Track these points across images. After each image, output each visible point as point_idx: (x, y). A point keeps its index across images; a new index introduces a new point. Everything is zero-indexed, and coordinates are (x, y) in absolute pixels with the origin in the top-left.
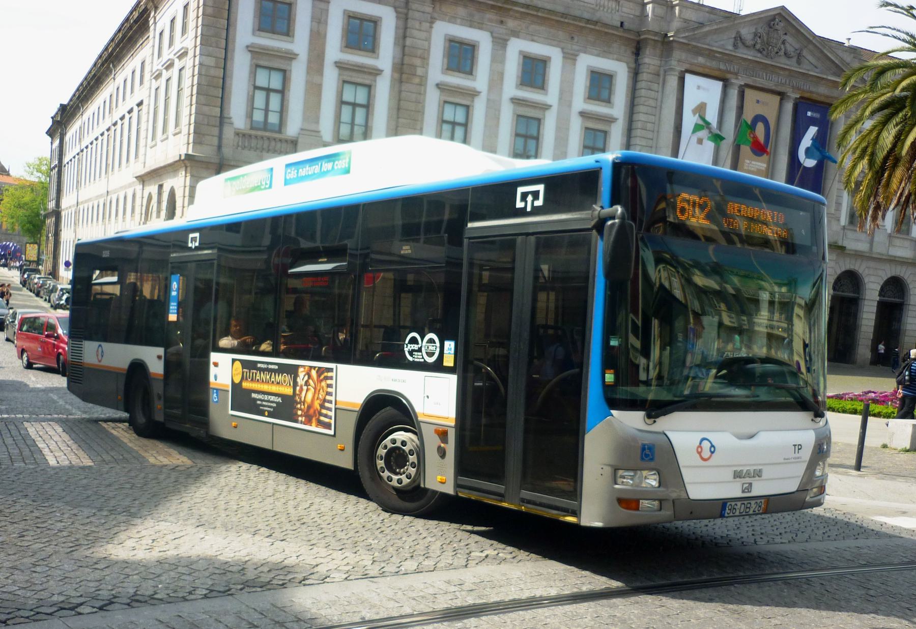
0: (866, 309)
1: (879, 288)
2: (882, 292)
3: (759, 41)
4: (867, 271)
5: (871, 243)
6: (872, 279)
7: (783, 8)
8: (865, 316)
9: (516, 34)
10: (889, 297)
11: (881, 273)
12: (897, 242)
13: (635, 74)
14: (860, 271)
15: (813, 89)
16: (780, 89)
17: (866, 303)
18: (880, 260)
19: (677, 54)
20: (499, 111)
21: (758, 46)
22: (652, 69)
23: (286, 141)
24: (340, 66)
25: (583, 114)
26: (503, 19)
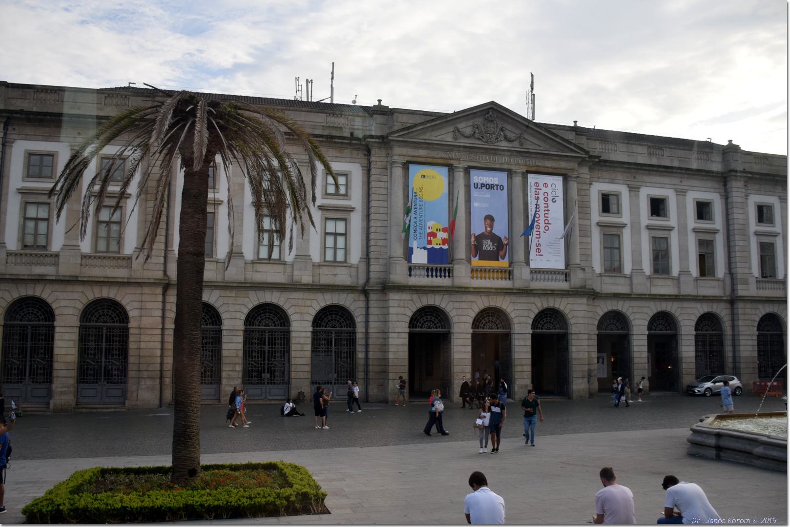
0: (635, 343)
1: (646, 323)
3: (477, 131)
5: (631, 285)
6: (638, 316)
7: (493, 103)
8: (635, 349)
10: (661, 330)
11: (645, 310)
12: (660, 282)
14: (624, 311)
16: (506, 167)
17: (635, 337)
18: (642, 297)
20: (242, 214)
21: (477, 135)
22: (379, 165)
23: (124, 258)
24: (23, 192)
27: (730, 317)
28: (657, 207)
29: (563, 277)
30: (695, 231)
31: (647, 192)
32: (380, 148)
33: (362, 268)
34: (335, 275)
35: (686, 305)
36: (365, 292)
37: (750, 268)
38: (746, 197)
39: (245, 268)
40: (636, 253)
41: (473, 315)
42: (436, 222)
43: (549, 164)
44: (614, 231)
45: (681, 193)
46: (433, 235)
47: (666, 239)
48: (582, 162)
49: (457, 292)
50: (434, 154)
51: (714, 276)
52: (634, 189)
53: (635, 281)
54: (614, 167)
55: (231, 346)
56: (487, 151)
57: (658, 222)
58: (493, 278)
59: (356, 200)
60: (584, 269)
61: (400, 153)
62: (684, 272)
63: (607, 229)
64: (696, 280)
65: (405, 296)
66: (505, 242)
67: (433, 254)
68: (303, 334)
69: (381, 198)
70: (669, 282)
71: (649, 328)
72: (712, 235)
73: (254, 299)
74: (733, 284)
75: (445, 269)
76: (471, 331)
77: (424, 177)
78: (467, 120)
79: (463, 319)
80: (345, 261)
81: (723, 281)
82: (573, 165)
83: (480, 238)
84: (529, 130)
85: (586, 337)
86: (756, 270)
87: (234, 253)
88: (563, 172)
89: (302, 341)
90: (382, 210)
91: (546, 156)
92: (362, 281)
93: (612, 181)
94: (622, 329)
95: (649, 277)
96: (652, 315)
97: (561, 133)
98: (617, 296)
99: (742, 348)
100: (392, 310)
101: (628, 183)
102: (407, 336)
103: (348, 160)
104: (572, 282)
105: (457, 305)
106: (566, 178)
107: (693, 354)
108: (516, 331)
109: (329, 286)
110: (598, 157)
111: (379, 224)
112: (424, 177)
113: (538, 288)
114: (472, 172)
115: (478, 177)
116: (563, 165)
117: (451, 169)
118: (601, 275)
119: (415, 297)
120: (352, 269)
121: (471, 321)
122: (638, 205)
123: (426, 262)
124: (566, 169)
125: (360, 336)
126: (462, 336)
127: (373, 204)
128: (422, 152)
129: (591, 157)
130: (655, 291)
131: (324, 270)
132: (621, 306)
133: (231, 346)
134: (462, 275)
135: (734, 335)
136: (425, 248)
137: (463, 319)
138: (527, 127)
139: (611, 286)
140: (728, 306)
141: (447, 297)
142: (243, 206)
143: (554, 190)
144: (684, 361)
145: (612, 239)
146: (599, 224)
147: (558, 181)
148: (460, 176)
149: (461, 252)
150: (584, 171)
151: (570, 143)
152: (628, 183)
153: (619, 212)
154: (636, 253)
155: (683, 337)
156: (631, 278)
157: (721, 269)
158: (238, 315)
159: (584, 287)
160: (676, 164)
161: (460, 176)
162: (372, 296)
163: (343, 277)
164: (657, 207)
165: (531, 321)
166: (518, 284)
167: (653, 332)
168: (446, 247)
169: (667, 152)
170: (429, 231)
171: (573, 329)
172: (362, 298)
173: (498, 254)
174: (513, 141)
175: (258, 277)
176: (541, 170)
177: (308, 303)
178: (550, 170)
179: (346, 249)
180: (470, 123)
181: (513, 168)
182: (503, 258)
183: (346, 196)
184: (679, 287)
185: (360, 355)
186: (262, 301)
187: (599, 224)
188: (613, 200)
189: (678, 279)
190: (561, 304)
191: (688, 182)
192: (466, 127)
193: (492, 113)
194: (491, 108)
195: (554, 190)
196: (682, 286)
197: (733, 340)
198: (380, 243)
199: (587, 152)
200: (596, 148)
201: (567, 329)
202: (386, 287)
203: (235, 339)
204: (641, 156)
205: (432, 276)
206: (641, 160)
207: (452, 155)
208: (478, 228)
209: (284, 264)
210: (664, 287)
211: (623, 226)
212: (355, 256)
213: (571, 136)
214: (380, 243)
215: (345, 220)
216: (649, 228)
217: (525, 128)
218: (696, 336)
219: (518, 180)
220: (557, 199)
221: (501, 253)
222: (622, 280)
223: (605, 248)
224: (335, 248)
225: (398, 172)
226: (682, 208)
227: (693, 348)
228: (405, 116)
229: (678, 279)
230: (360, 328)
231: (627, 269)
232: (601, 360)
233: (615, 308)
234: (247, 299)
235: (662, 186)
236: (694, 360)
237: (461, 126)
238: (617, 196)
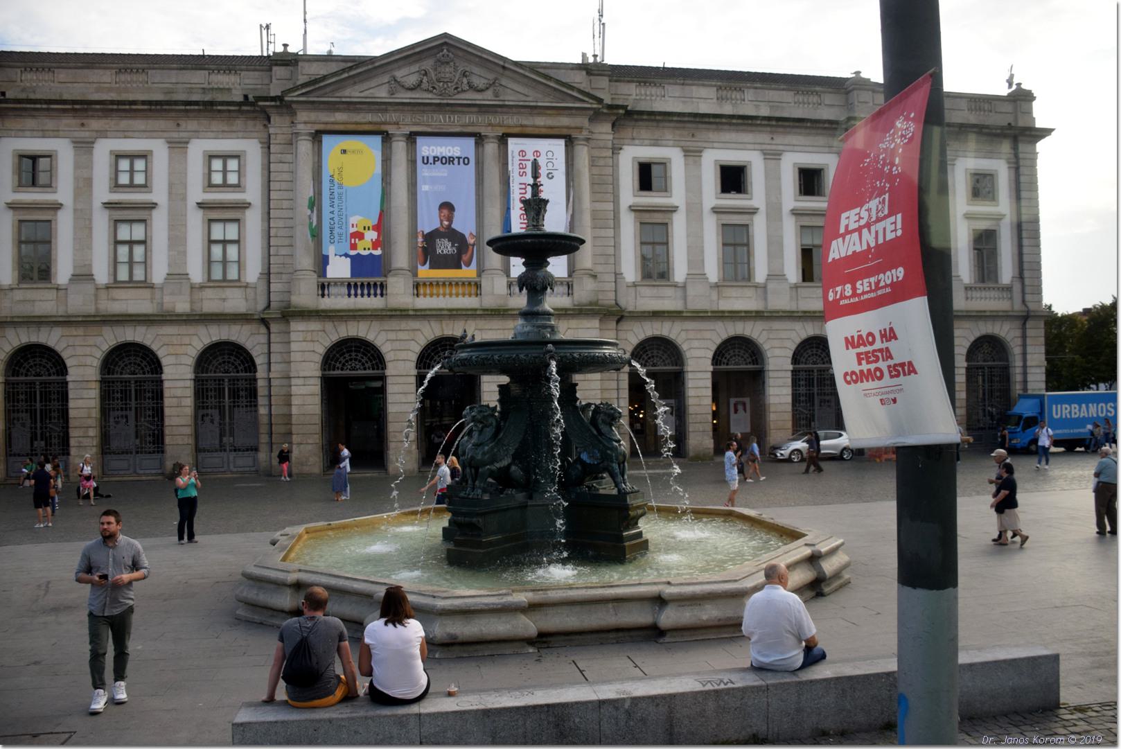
1: (710, 354)
2: (796, 359)
4: (683, 335)
5: (685, 298)
6: (696, 344)
7: (446, 35)
9: (103, 134)
10: (736, 364)
11: (708, 335)
12: (733, 292)
13: (267, 145)
15: (525, 122)
19: (302, 116)
20: (90, 220)
21: (425, 85)
22: (280, 139)
25: (201, 205)
26: (84, 121)
27: (1019, 341)
28: (733, 179)
30: (716, 211)
31: (714, 157)
32: (281, 114)
33: (262, 288)
34: (224, 300)
35: (777, 325)
36: (265, 322)
38: (616, 150)
39: (96, 296)
40: (695, 249)
41: (418, 349)
42: (361, 218)
43: (541, 121)
44: (658, 218)
45: (772, 156)
46: (360, 236)
47: (49, 221)
48: (596, 116)
49: (118, 321)
50: (359, 117)
51: (997, 282)
52: (693, 154)
53: (691, 291)
54: (658, 121)
55: (80, 403)
56: (440, 107)
57: (733, 200)
58: (451, 295)
59: (253, 193)
60: (595, 277)
61: (306, 120)
62: (776, 276)
63: (647, 215)
64: (796, 287)
65: (314, 325)
66: (471, 241)
67: (359, 263)
68: (181, 384)
69: (284, 186)
70: (749, 292)
71: (968, 360)
72: (146, 212)
73: (110, 338)
75: (369, 284)
77: (344, 152)
78: (410, 64)
79: (403, 355)
80: (239, 280)
82: (583, 121)
83: (431, 237)
84: (507, 73)
87: (83, 276)
88: (565, 132)
89: (179, 393)
90: (286, 204)
91: (534, 110)
92: (261, 305)
93: (656, 143)
94: (755, 362)
95: (717, 286)
96: (719, 341)
97: (552, 73)
98: (656, 315)
100: (294, 346)
101: (683, 144)
102: (318, 382)
103: (240, 134)
104: (576, 294)
105: (392, 336)
106: (570, 141)
107: (789, 399)
108: (689, 369)
109: (217, 315)
110: (624, 107)
111: (281, 223)
112: (344, 152)
113: (345, 307)
114: (420, 140)
115: (427, 148)
116: (565, 121)
117: (387, 138)
118: (635, 285)
119: (329, 326)
120: (249, 290)
121: (414, 357)
122: (699, 178)
123: (349, 275)
124: (568, 128)
125: (261, 383)
126: (699, 375)
127: (273, 195)
128: (340, 117)
129: (610, 107)
130: (725, 305)
131: (208, 293)
132: (52, 338)
133: (80, 403)
134: (399, 292)
136: (346, 255)
137: (403, 355)
138: (504, 67)
139: (650, 299)
140: (1018, 323)
141: (376, 325)
142: (91, 210)
143: (550, 161)
144: (772, 409)
145: (655, 230)
146: (634, 209)
147: (558, 146)
148: (400, 147)
149: (401, 257)
150: (604, 131)
151: (572, 88)
152: (683, 144)
153: (666, 189)
154: (695, 249)
155: (771, 374)
156: (684, 287)
158: (89, 360)
159: (596, 303)
160: (764, 111)
161: (400, 147)
162: (274, 327)
163: (235, 302)
164: (733, 179)
166: (488, 301)
168: (378, 252)
169: (749, 94)
170: (352, 230)
172: (263, 330)
173: (459, 259)
174: (481, 91)
175: (117, 308)
176: (529, 131)
177: (186, 340)
178: (544, 131)
179: (240, 263)
180: (415, 68)
181: (483, 131)
182: (468, 265)
183: (145, 187)
184: (766, 299)
185: (263, 411)
186: (121, 340)
187: (634, 209)
188: (655, 171)
191: (781, 140)
192: (408, 75)
193: (444, 51)
194: (445, 43)
195: (550, 161)
196: (770, 296)
198: (283, 251)
199: (600, 101)
200: (632, 95)
202: (289, 314)
203: (85, 394)
204: (705, 101)
205: (356, 295)
206: (704, 108)
207: (387, 117)
208: (429, 221)
209: (152, 287)
211: (672, 210)
212: (253, 273)
213: (579, 79)
214: (283, 251)
215: (144, 221)
216: (716, 211)
217: (501, 70)
218: (794, 372)
219: (491, 148)
220: (555, 173)
221: (465, 258)
222: (669, 292)
223: (724, 245)
224: (131, 263)
225: (305, 147)
226: (773, 179)
227: (789, 391)
228: (315, 65)
230: (261, 373)
231: (680, 272)
232: (740, 407)
234: (101, 338)
235: (741, 146)
236: (789, 408)
237: (399, 74)
238: (664, 164)
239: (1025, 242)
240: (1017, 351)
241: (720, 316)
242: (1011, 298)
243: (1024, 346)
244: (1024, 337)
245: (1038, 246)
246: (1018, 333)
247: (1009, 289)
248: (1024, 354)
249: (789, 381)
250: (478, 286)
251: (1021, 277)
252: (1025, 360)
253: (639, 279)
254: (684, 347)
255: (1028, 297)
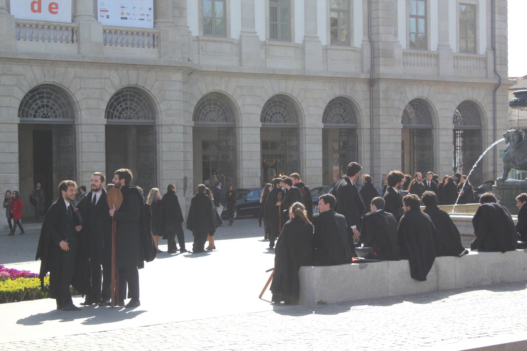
1: (259, 111)
10: (277, 121)
17: (244, 131)
29: (148, 40)
37: (396, 34)
41: (21, 96)
64: (326, 49)
74: (374, 57)
76: (17, 120)
81: (361, 52)
85: (181, 129)
86: (402, 40)
95: (264, 44)
96: (267, 99)
99: (382, 147)
135: (372, 129)
155: (308, 131)
157: (359, 37)
165: (104, 107)
167: (268, 123)
171: (163, 118)
189: (302, 48)
190: (150, 83)
197: (371, 135)
201: (154, 118)
210: (282, 60)
229: (302, 48)
233: (217, 88)
239: (497, 17)
240: (489, 115)
241: (271, 76)
242: (486, 68)
243: (494, 111)
244: (494, 103)
245: (505, 21)
246: (490, 99)
247: (485, 60)
248: (494, 118)
249: (320, 138)
250: (74, 31)
251: (494, 49)
252: (494, 124)
253: (202, 34)
254: (239, 103)
255: (498, 67)
